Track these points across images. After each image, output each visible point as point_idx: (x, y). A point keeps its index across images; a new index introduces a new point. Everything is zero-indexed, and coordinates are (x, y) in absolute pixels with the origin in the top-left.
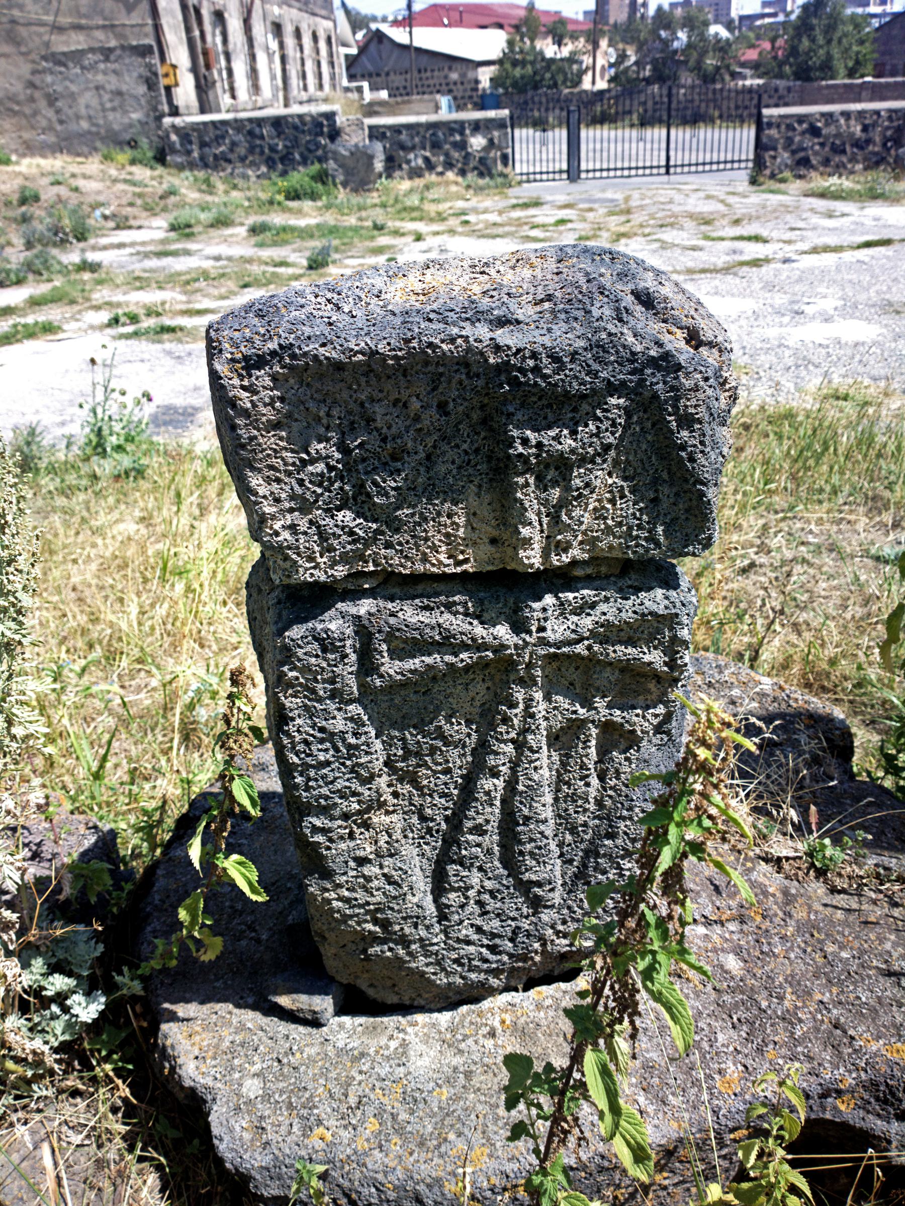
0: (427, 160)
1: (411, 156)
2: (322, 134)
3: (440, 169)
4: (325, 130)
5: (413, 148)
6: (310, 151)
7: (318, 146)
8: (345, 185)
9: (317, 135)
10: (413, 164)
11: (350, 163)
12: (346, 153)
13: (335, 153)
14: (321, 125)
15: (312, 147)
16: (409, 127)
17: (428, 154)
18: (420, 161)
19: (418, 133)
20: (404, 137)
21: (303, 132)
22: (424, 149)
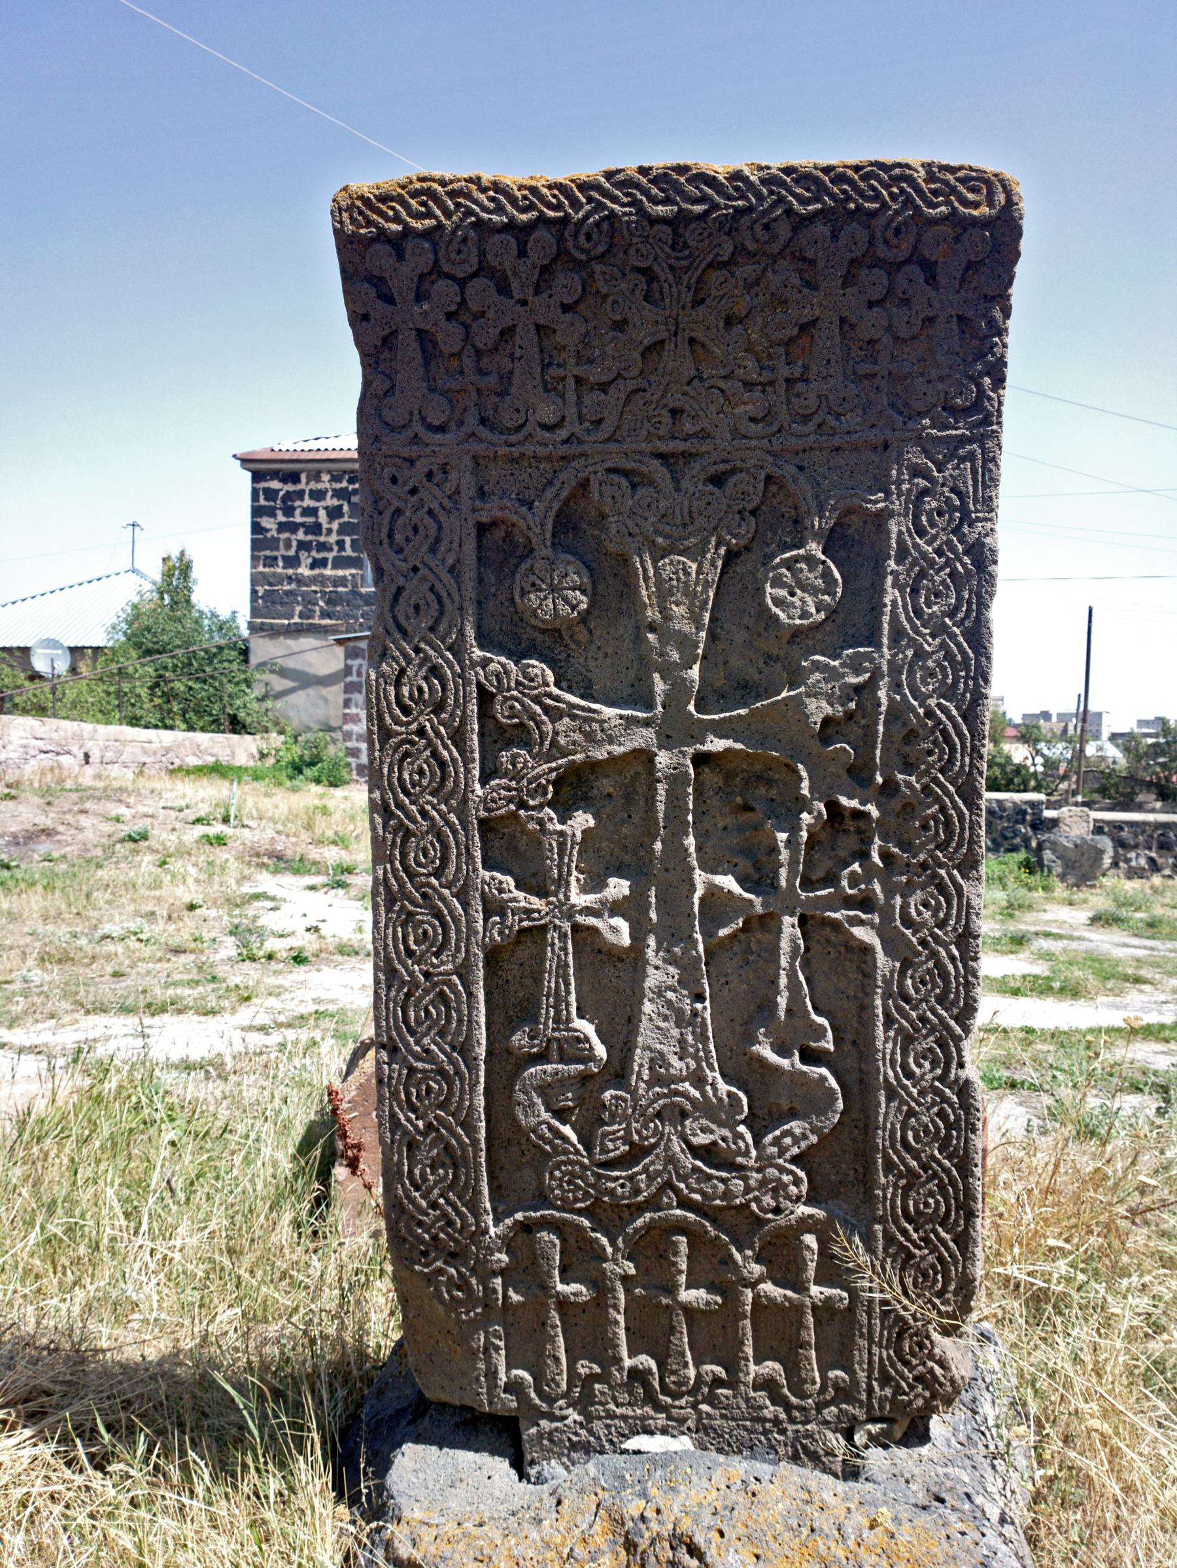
0: (1151, 861)
1: (1132, 855)
2: (1023, 821)
3: (1167, 872)
4: (1028, 818)
5: (1136, 846)
6: (1006, 838)
7: (1016, 833)
8: (1062, 877)
9: (1017, 822)
10: (1133, 864)
11: (1072, 856)
12: (1071, 845)
13: (1054, 843)
14: (1025, 812)
15: (1009, 835)
16: (1132, 824)
17: (1153, 855)
18: (1143, 862)
19: (1144, 832)
20: (1124, 834)
21: (1001, 818)
22: (1150, 849)
